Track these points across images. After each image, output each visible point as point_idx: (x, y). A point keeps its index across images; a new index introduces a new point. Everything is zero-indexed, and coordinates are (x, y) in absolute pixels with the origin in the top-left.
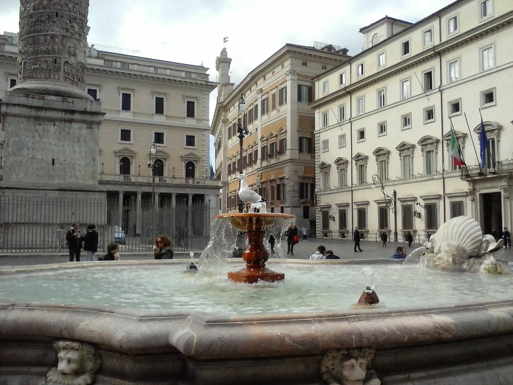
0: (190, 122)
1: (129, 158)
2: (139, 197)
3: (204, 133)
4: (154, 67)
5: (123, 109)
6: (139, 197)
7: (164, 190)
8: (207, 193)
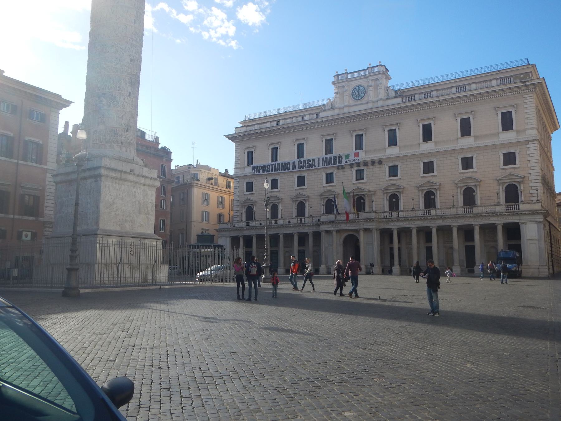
0: (509, 136)
1: (433, 190)
2: (414, 232)
3: (528, 146)
4: (456, 86)
5: (424, 141)
6: (414, 232)
7: (441, 223)
8: (523, 221)
